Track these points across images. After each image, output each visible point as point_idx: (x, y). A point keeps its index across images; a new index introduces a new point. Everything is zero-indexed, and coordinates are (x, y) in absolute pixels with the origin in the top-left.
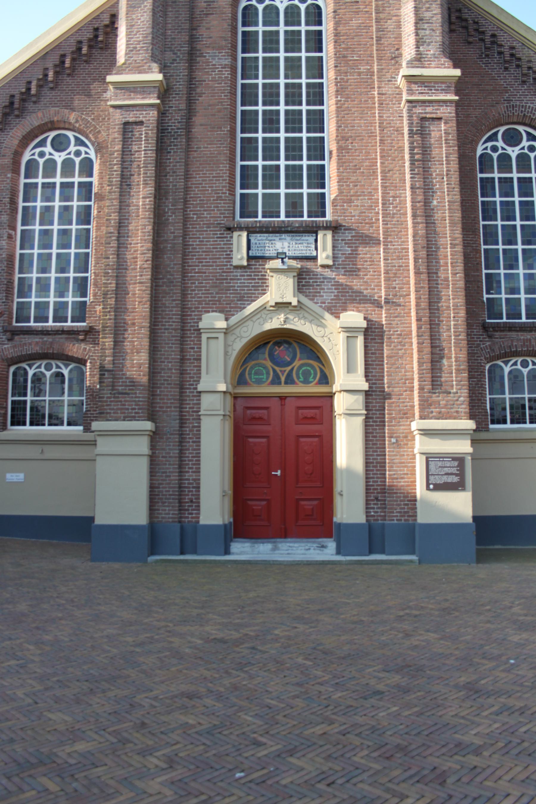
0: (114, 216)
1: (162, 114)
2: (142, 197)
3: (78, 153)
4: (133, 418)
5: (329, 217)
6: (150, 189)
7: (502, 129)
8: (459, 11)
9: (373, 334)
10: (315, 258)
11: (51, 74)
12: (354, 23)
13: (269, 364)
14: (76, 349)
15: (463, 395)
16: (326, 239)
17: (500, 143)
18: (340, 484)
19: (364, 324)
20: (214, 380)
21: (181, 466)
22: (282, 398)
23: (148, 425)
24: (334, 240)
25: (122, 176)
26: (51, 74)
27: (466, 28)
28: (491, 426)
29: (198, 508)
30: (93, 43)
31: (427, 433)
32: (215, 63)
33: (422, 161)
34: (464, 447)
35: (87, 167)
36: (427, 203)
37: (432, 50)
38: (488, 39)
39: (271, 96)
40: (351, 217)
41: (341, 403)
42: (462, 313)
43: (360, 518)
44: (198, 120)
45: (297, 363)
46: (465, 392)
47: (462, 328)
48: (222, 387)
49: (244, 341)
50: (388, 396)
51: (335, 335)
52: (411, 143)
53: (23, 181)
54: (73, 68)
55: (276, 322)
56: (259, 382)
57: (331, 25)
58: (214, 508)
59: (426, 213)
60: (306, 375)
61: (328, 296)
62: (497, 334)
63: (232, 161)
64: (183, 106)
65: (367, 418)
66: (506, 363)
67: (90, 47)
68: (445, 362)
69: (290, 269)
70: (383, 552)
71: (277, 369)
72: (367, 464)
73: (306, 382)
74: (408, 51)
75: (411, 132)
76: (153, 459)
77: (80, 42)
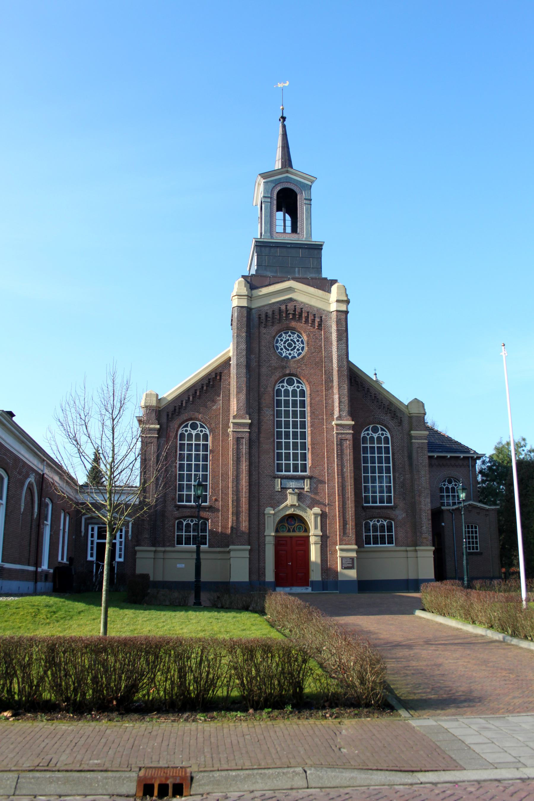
0: (235, 473)
1: (250, 433)
2: (244, 466)
3: (201, 431)
4: (244, 545)
5: (307, 473)
6: (247, 463)
7: (371, 426)
8: (355, 377)
9: (323, 516)
10: (304, 489)
11: (191, 398)
12: (317, 399)
13: (286, 525)
14: (203, 514)
15: (354, 537)
16: (307, 482)
17: (370, 432)
18: (312, 567)
19: (321, 512)
20: (270, 532)
21: (259, 561)
22: (291, 537)
23: (249, 547)
24: (310, 482)
25: (237, 458)
26: (191, 398)
27: (358, 384)
28: (365, 546)
29: (265, 576)
30: (208, 385)
31: (341, 550)
32: (267, 413)
33: (341, 455)
34: (354, 555)
35: (206, 437)
36: (342, 470)
37: (344, 414)
38: (366, 390)
39: (287, 425)
40: (316, 474)
41: (312, 540)
42: (354, 509)
43: (319, 578)
44: (262, 435)
45: (296, 525)
46: (354, 536)
47: (353, 515)
48: (273, 534)
49: (280, 518)
50: (328, 537)
51: (311, 516)
52: (337, 448)
53: (179, 442)
54: (200, 395)
55: (291, 511)
56: (283, 531)
57: (309, 399)
58: (270, 576)
59: (342, 474)
60: (300, 528)
61: (308, 502)
62: (368, 510)
63: (274, 451)
64: (257, 431)
65: (322, 544)
66: (371, 521)
67: (207, 386)
68: (347, 526)
69: (296, 493)
70: (327, 590)
71: (290, 527)
72: (322, 560)
73: (299, 531)
74: (336, 414)
75: (337, 444)
76: (250, 558)
77: (203, 384)
